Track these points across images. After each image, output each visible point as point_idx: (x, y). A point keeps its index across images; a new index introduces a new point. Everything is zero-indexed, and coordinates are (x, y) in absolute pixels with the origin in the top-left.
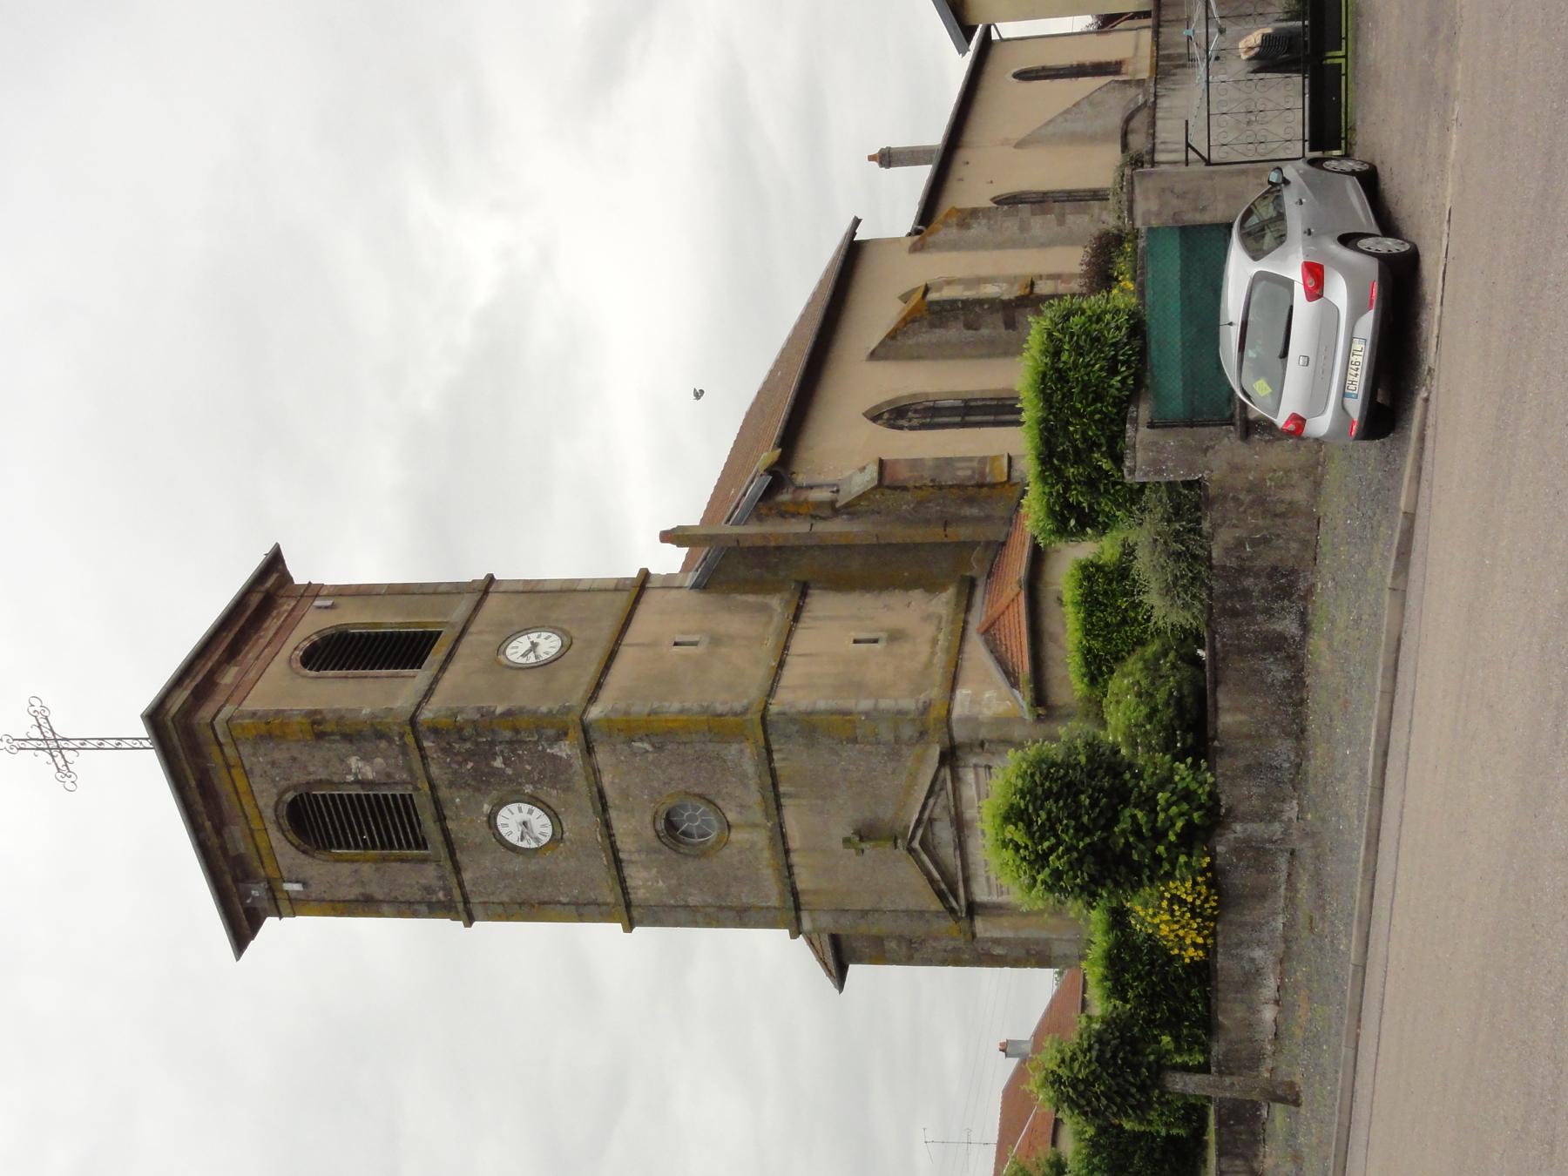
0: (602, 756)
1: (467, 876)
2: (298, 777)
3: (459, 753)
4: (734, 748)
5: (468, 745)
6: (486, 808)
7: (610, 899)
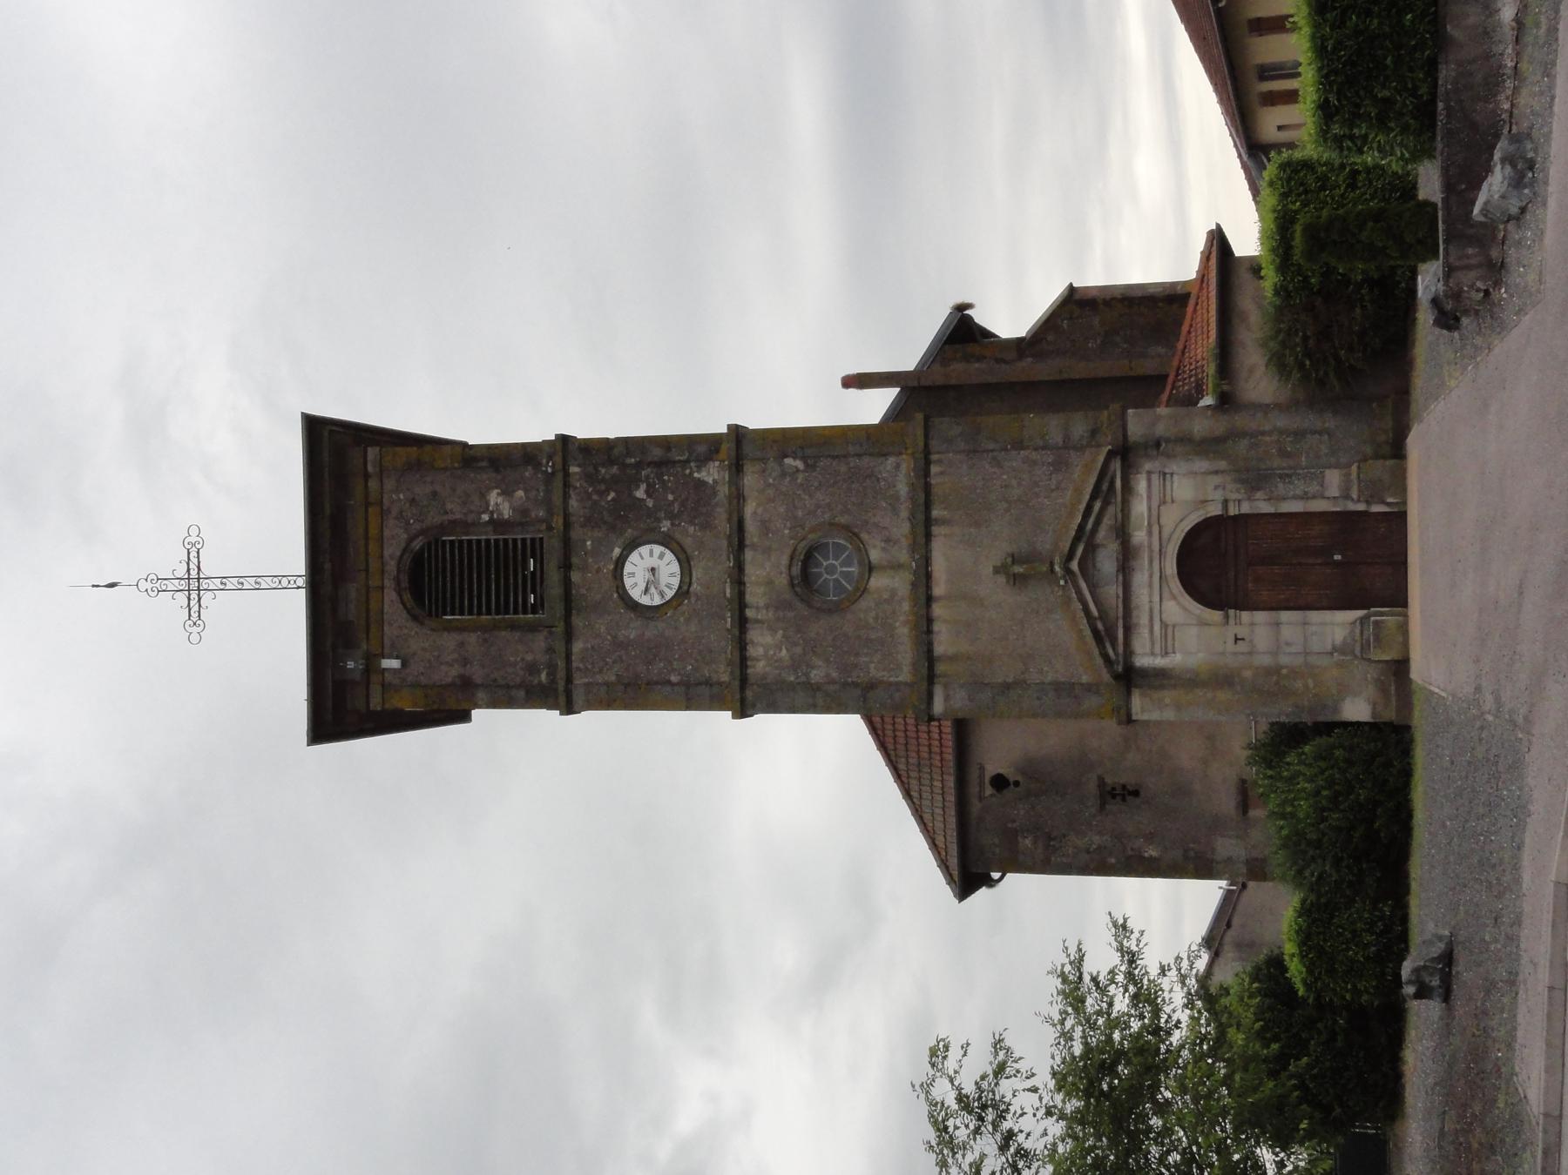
0: (750, 480)
1: (577, 646)
2: (433, 518)
3: (603, 480)
4: (891, 460)
5: (615, 469)
6: (617, 551)
7: (725, 678)
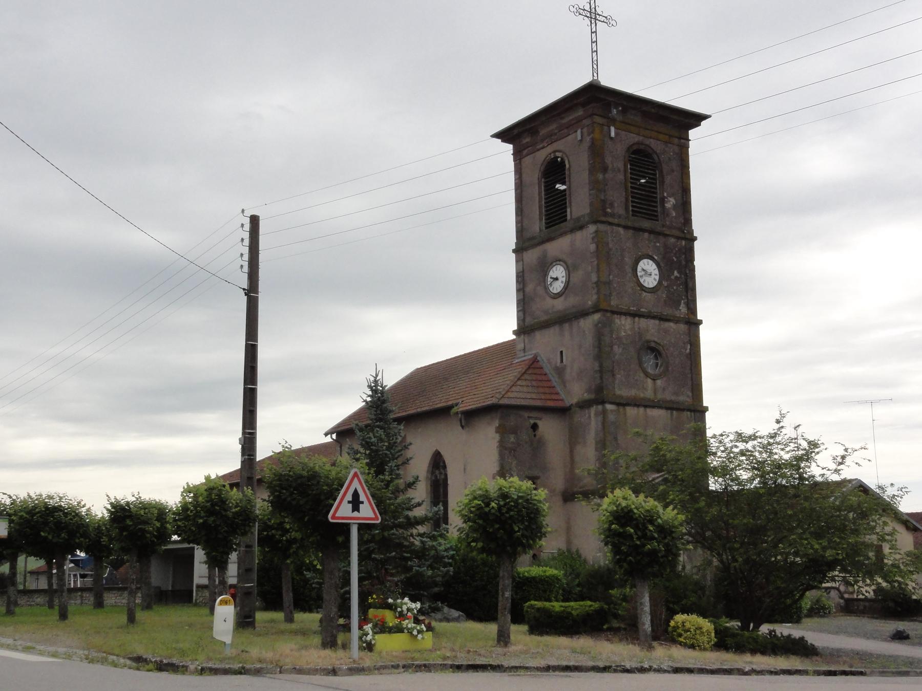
1: (621, 230)
